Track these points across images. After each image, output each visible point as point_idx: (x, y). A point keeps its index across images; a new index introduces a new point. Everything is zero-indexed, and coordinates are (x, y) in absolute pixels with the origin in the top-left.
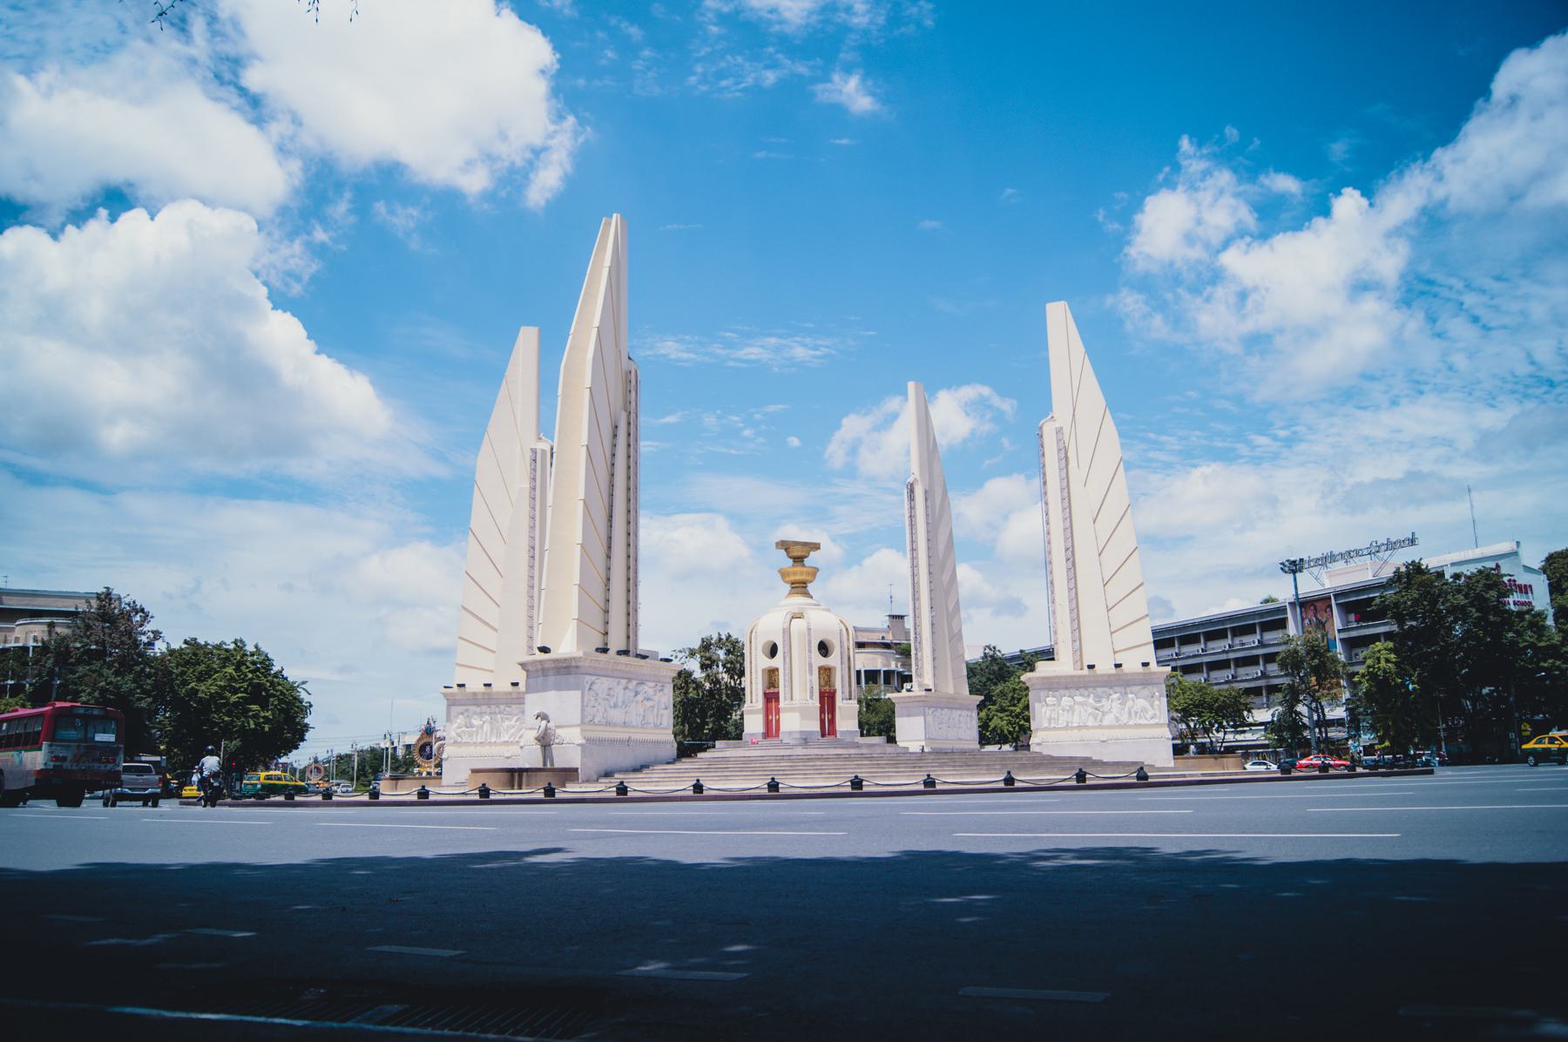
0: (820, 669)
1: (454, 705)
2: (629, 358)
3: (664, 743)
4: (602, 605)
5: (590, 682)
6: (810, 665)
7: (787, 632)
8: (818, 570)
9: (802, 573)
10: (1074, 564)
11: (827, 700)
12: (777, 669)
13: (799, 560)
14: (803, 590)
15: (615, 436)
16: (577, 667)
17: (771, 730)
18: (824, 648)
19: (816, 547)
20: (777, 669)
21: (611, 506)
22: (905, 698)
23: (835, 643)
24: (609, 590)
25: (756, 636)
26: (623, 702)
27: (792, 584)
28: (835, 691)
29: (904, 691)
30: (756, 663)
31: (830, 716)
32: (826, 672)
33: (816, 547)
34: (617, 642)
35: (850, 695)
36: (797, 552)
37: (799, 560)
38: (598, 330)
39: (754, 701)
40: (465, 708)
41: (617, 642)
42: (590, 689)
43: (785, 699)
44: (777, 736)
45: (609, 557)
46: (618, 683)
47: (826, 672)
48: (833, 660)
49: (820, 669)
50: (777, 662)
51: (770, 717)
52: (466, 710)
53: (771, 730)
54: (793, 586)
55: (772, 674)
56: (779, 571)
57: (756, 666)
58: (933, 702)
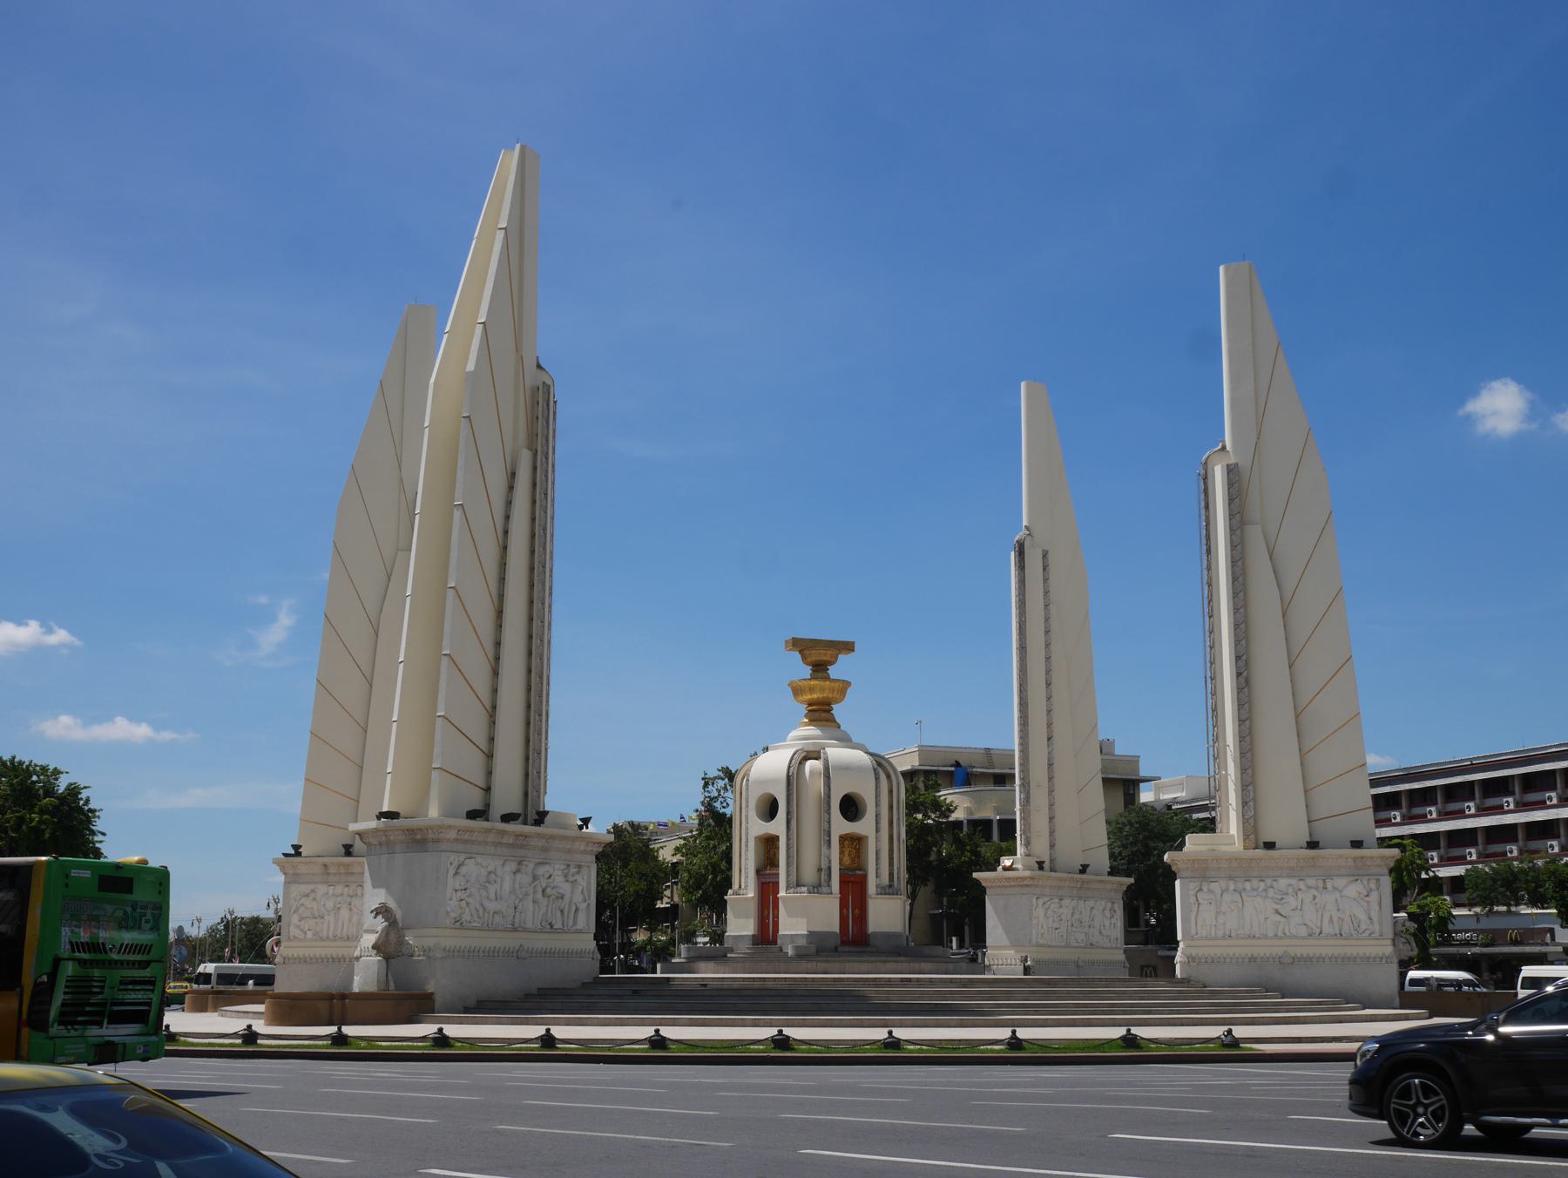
0: (843, 839)
1: (295, 882)
2: (539, 366)
3: (580, 954)
4: (484, 745)
5: (456, 864)
7: (793, 780)
8: (849, 684)
9: (822, 689)
10: (1247, 681)
11: (853, 888)
13: (820, 668)
14: (824, 715)
15: (511, 488)
16: (436, 841)
17: (766, 935)
19: (848, 647)
21: (501, 596)
22: (1000, 880)
23: (868, 794)
24: (494, 723)
25: (747, 785)
27: (810, 705)
28: (865, 877)
30: (750, 829)
33: (848, 647)
37: (820, 668)
38: (485, 328)
39: (743, 887)
40: (311, 887)
41: (507, 797)
42: (456, 873)
44: (774, 942)
45: (496, 673)
47: (853, 844)
48: (864, 827)
49: (843, 839)
50: (777, 827)
51: (766, 911)
52: (313, 891)
53: (766, 935)
55: (769, 843)
56: (789, 685)
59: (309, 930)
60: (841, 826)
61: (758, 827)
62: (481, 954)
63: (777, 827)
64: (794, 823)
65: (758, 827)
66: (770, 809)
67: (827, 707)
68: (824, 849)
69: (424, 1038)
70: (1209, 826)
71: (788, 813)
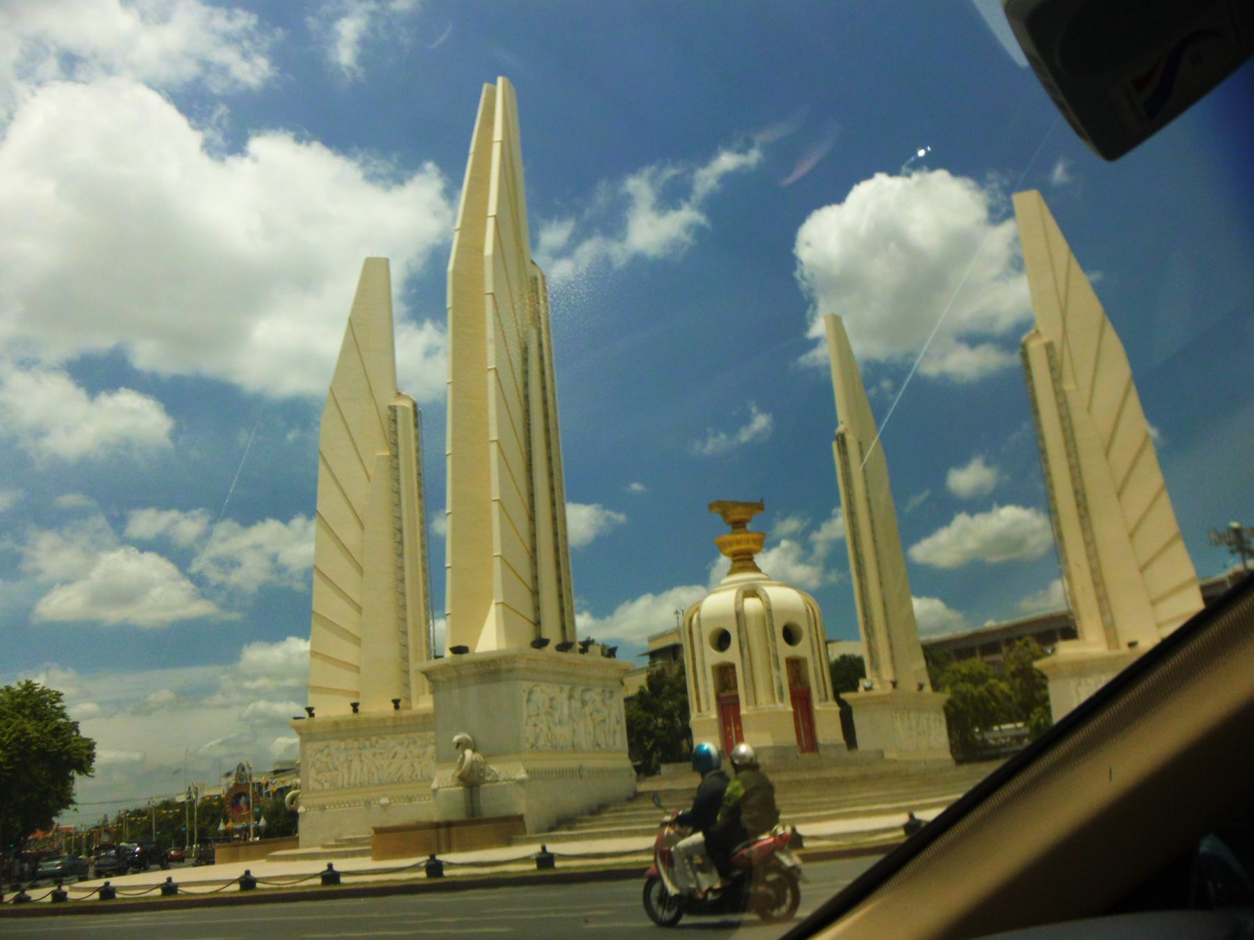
1: (309, 740)
3: (614, 772)
5: (527, 690)
6: (776, 658)
9: (748, 541)
12: (732, 666)
14: (750, 564)
16: (510, 671)
18: (790, 635)
20: (732, 666)
26: (570, 716)
29: (861, 689)
31: (806, 724)
32: (796, 666)
34: (552, 632)
35: (826, 695)
36: (737, 514)
40: (325, 743)
42: (528, 700)
43: (747, 704)
46: (561, 689)
47: (796, 666)
48: (802, 649)
50: (732, 655)
51: (728, 729)
52: (326, 746)
54: (737, 558)
57: (703, 663)
58: (894, 702)
59: (326, 782)
60: (785, 650)
61: (714, 657)
62: (554, 776)
63: (732, 655)
64: (745, 651)
65: (714, 657)
66: (722, 640)
67: (748, 557)
68: (775, 673)
69: (526, 860)
70: (1070, 632)
71: (740, 643)
